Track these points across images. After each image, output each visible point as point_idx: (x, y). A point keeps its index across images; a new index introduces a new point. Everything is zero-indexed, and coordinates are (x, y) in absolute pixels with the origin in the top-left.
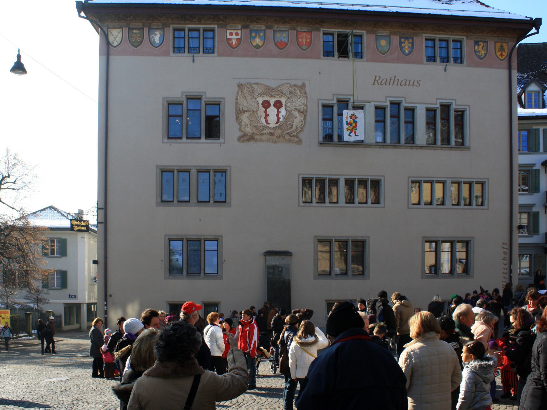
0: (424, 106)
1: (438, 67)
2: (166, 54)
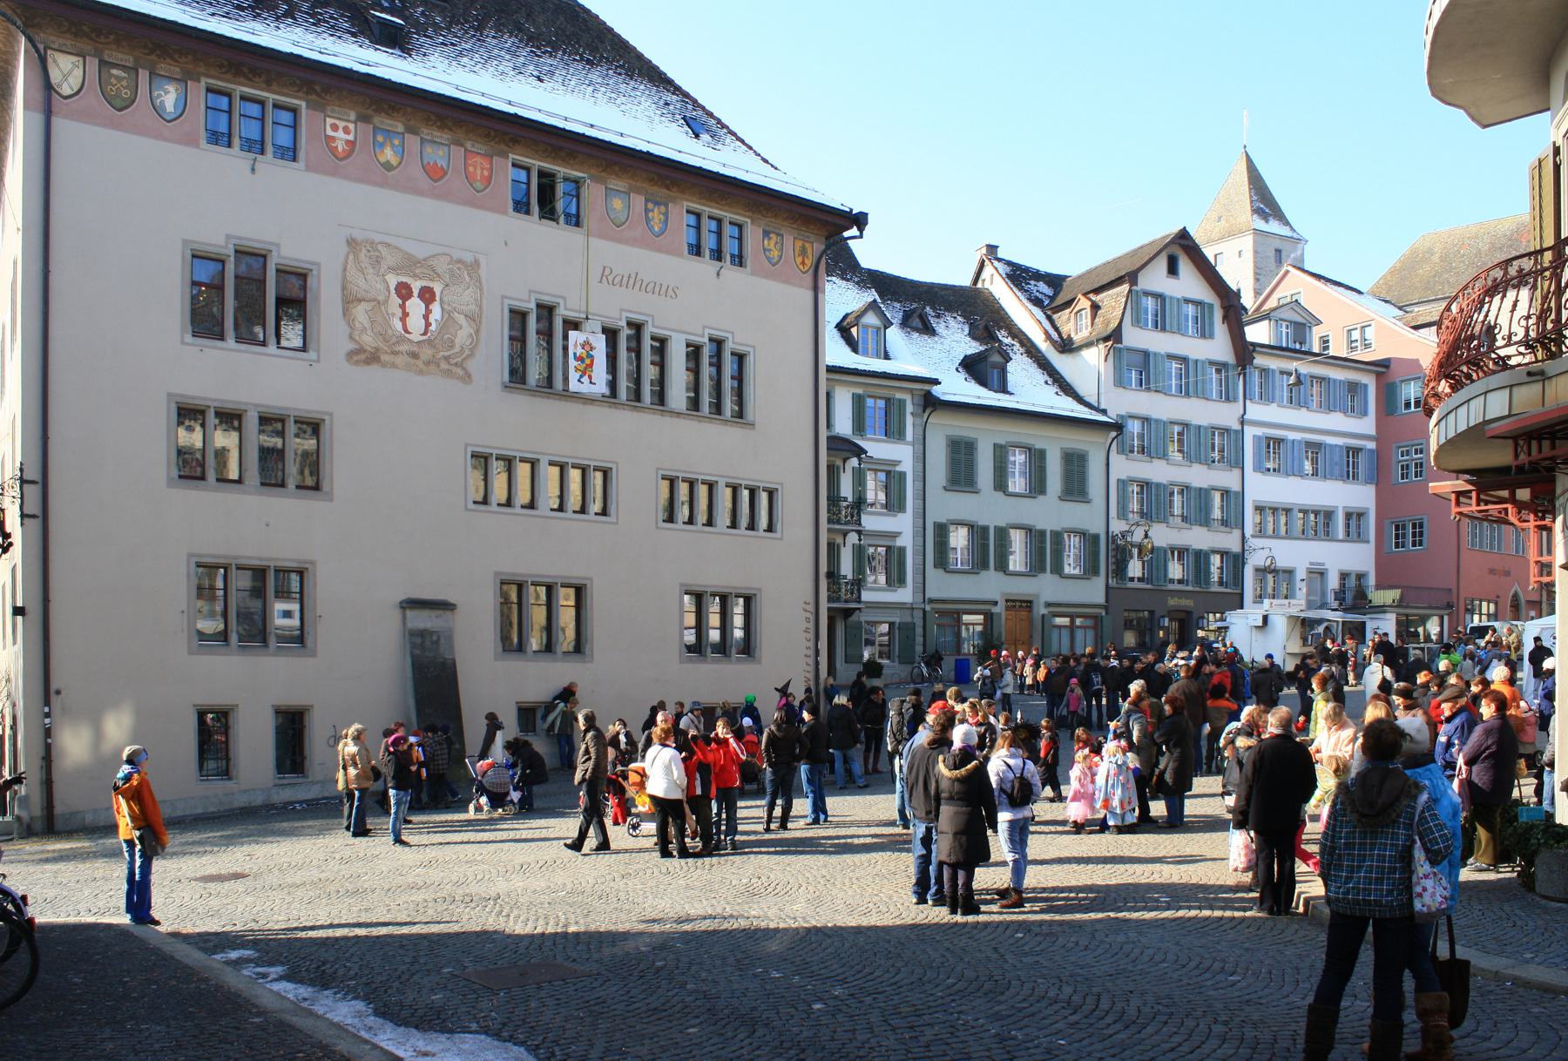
0: (684, 337)
1: (704, 267)
2: (192, 142)
